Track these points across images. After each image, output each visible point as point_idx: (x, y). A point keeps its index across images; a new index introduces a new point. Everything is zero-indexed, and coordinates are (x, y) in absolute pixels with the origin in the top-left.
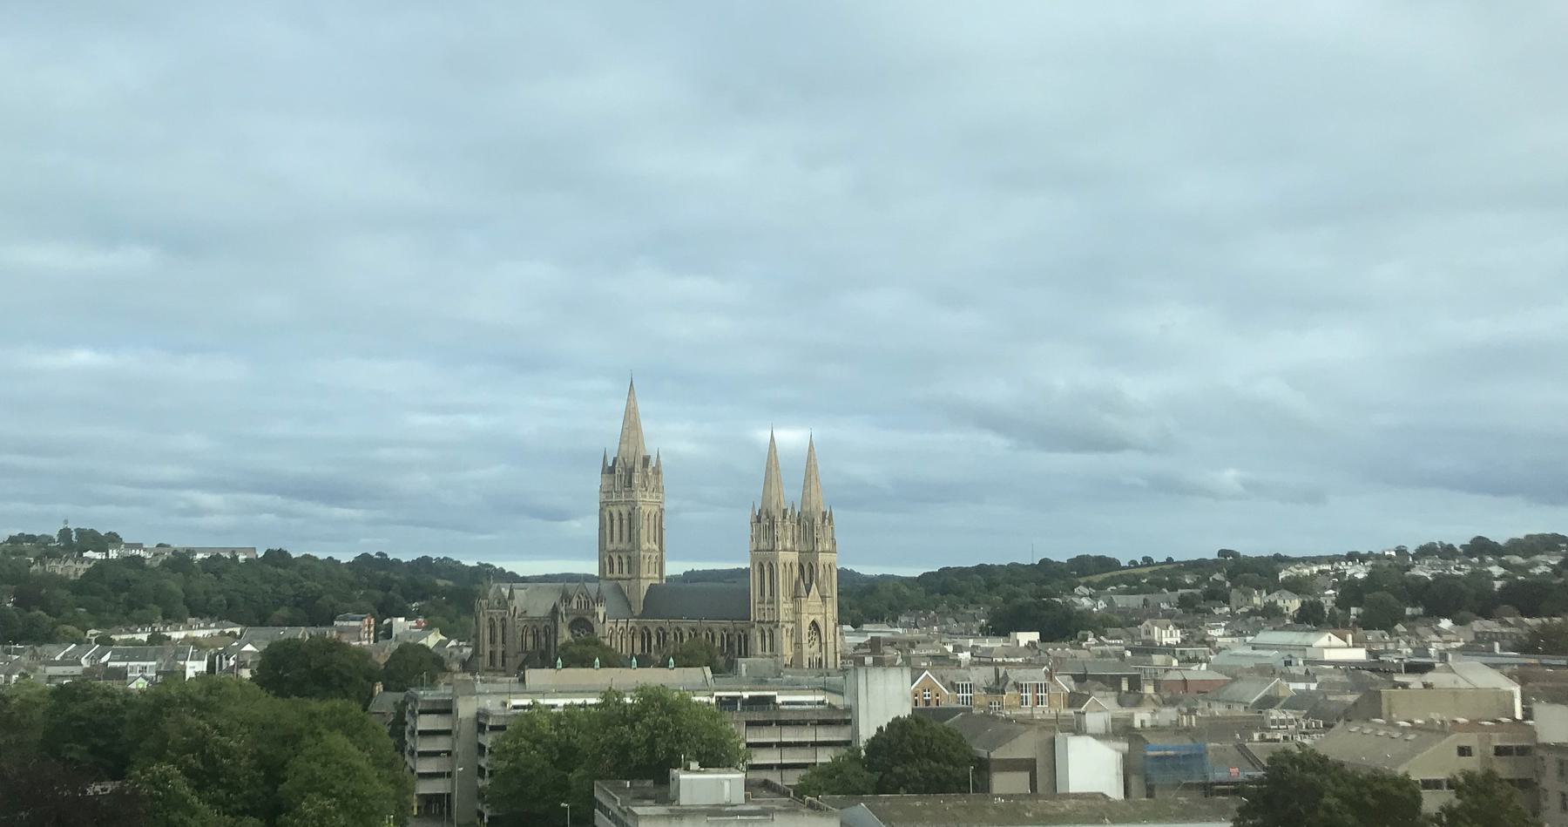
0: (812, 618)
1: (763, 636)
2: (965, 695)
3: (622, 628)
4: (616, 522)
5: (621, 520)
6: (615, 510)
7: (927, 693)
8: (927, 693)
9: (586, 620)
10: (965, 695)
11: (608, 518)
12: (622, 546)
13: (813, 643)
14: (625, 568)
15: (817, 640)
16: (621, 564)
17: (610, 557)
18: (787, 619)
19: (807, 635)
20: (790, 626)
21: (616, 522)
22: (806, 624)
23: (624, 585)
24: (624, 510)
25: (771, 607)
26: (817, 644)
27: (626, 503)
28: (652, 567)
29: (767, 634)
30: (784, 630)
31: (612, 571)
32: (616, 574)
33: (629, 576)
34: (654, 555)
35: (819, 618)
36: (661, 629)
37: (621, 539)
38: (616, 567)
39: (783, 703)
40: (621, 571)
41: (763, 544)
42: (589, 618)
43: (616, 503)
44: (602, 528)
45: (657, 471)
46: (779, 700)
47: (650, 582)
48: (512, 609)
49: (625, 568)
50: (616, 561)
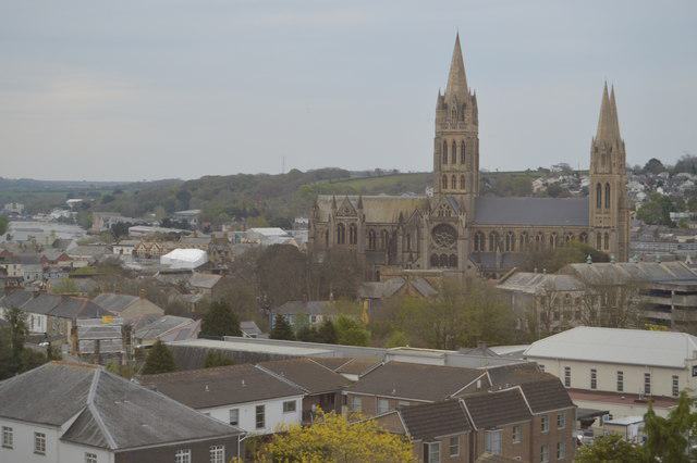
1: (599, 238)
4: (450, 149)
5: (454, 146)
6: (449, 140)
9: (449, 226)
12: (456, 167)
14: (458, 184)
16: (454, 181)
17: (445, 176)
21: (450, 149)
24: (458, 140)
27: (462, 133)
32: (449, 189)
33: (463, 191)
36: (493, 232)
37: (454, 161)
38: (449, 184)
40: (454, 187)
41: (600, 170)
42: (452, 223)
43: (451, 133)
49: (458, 184)
50: (449, 179)
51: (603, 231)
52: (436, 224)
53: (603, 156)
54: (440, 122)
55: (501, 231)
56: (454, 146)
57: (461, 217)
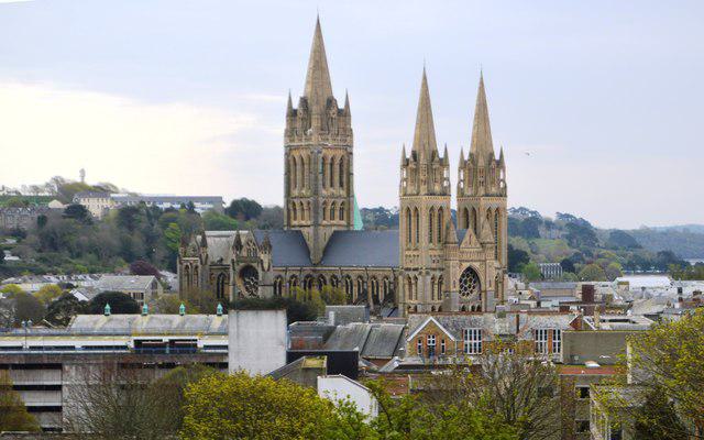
0: (466, 265)
2: (473, 341)
3: (293, 276)
4: (299, 167)
5: (303, 164)
6: (296, 154)
7: (432, 339)
8: (432, 339)
10: (473, 341)
11: (292, 163)
13: (471, 292)
15: (477, 288)
17: (294, 204)
18: (434, 266)
19: (457, 282)
20: (438, 274)
21: (299, 167)
22: (456, 272)
23: (305, 231)
24: (304, 153)
25: (416, 253)
26: (475, 292)
28: (337, 213)
29: (413, 282)
30: (429, 278)
31: (295, 219)
33: (309, 223)
34: (339, 202)
35: (476, 265)
38: (299, 214)
39: (206, 347)
42: (255, 265)
43: (297, 148)
44: (288, 173)
45: (344, 114)
46: (200, 344)
47: (334, 228)
48: (204, 258)
51: (412, 274)
52: (242, 264)
53: (412, 170)
54: (291, 133)
55: (339, 275)
56: (303, 164)
57: (262, 256)
